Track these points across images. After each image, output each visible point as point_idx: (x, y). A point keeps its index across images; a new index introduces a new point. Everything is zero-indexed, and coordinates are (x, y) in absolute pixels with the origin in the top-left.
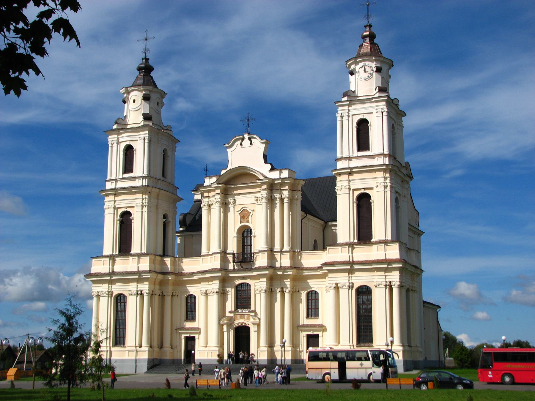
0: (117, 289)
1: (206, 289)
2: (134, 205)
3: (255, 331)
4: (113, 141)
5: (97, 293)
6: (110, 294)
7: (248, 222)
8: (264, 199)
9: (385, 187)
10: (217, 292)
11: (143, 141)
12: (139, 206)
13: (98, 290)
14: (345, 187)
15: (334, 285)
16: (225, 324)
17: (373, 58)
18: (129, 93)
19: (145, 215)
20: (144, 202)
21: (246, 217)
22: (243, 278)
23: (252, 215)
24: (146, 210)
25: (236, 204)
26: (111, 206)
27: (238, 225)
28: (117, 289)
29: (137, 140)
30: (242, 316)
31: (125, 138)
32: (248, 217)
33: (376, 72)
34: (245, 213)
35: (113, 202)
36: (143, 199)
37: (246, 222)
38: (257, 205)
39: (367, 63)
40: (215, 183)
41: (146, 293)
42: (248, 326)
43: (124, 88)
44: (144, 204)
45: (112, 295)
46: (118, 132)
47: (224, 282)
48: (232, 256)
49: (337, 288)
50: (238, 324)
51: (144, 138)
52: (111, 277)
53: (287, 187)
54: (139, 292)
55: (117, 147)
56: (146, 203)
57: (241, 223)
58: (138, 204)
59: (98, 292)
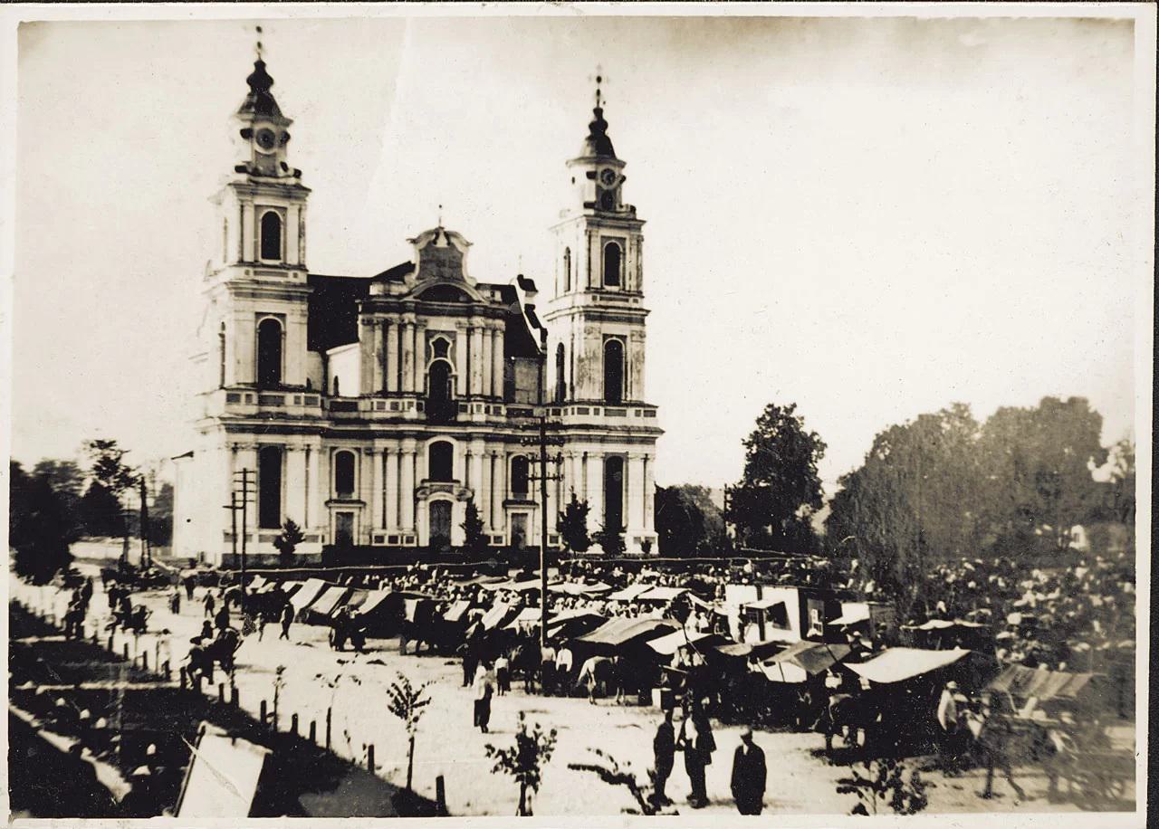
1: (385, 446)
7: (446, 357)
15: (583, 455)
27: (433, 360)
54: (306, 448)
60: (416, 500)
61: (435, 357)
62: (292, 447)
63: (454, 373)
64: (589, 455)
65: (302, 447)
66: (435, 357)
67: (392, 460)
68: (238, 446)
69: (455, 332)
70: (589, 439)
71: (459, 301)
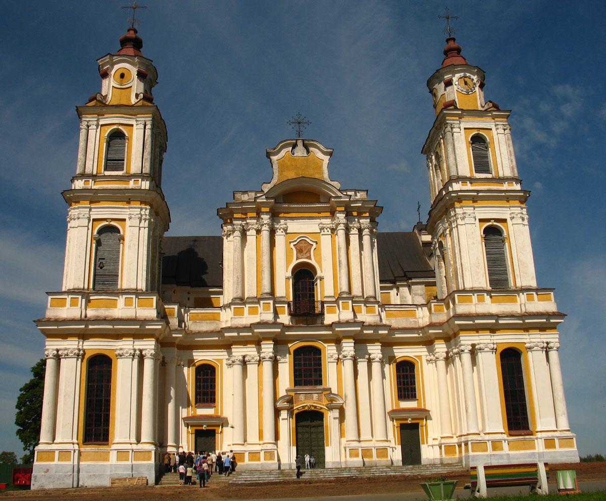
0: (93, 346)
2: (126, 217)
3: (335, 418)
4: (89, 121)
5: (55, 352)
6: (81, 355)
7: (309, 258)
8: (341, 225)
9: (523, 219)
10: (270, 358)
11: (142, 126)
12: (135, 219)
13: (58, 347)
14: (469, 215)
15: (470, 348)
16: (284, 409)
17: (476, 70)
18: (113, 65)
19: (145, 233)
20: (143, 213)
21: (306, 251)
23: (315, 248)
24: (146, 224)
25: (288, 232)
26: (84, 216)
27: (295, 262)
28: (93, 346)
29: (132, 125)
30: (309, 396)
31: (113, 120)
32: (309, 251)
33: (479, 86)
34: (303, 245)
35: (88, 210)
36: (141, 209)
37: (305, 258)
38: (322, 235)
39: (468, 75)
40: (264, 197)
41: (151, 355)
42: (321, 410)
43: (109, 56)
44: (144, 217)
45: (84, 355)
46: (100, 110)
47: (280, 342)
48: (286, 306)
49: (474, 352)
50: (304, 407)
51: (145, 123)
52: (87, 326)
53: (367, 214)
55: (96, 131)
56: (146, 215)
57: (297, 259)
58: (133, 216)
59: (58, 351)
60: (277, 412)
62: (121, 352)
63: (319, 274)
64: (477, 347)
65: (132, 352)
66: (297, 259)
67: (252, 369)
68: (60, 353)
70: (477, 329)
71: (320, 202)
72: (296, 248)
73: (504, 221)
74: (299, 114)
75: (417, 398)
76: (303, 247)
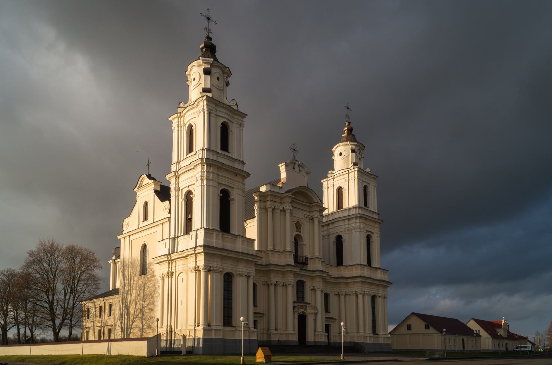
1: (277, 280)
5: (209, 268)
7: (300, 232)
22: (302, 276)
27: (295, 233)
32: (301, 227)
38: (306, 221)
50: (301, 312)
61: (296, 232)
66: (296, 232)
67: (279, 289)
69: (304, 219)
72: (296, 225)
73: (373, 233)
74: (294, 144)
75: (329, 312)
76: (298, 226)
